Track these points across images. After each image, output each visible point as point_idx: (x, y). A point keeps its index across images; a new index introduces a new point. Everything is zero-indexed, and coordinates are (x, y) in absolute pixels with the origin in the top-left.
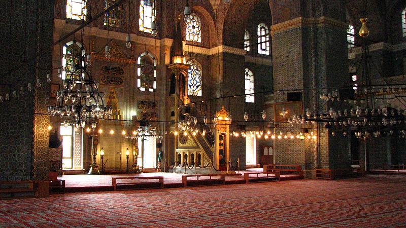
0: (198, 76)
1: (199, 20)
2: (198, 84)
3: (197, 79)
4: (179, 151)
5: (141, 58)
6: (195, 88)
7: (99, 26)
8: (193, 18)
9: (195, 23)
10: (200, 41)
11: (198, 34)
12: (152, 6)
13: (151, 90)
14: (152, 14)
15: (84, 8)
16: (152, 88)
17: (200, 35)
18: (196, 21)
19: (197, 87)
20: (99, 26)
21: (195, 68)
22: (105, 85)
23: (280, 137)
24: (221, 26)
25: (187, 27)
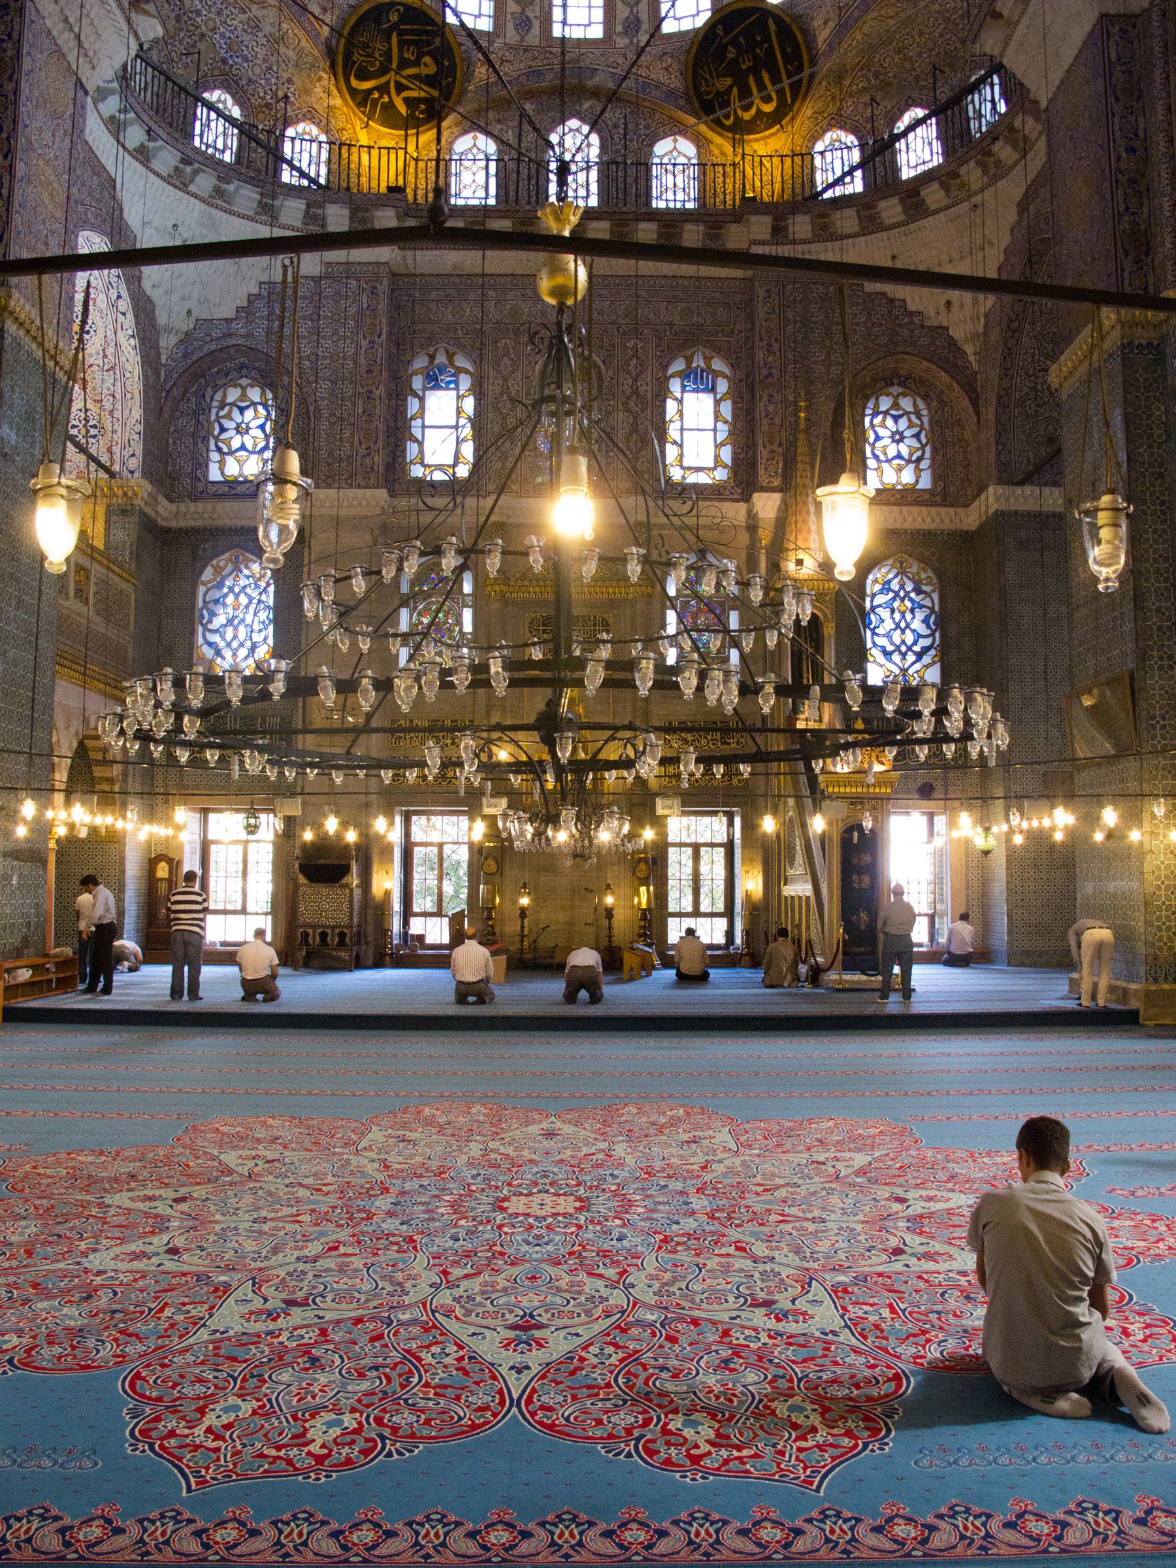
0: (920, 615)
1: (921, 405)
2: (925, 642)
3: (917, 625)
4: (789, 890)
6: (911, 658)
8: (896, 406)
9: (903, 423)
10: (925, 483)
11: (919, 460)
12: (713, 390)
14: (717, 416)
15: (465, 440)
17: (925, 464)
18: (908, 413)
19: (919, 656)
21: (909, 587)
24: (990, 413)
25: (866, 440)
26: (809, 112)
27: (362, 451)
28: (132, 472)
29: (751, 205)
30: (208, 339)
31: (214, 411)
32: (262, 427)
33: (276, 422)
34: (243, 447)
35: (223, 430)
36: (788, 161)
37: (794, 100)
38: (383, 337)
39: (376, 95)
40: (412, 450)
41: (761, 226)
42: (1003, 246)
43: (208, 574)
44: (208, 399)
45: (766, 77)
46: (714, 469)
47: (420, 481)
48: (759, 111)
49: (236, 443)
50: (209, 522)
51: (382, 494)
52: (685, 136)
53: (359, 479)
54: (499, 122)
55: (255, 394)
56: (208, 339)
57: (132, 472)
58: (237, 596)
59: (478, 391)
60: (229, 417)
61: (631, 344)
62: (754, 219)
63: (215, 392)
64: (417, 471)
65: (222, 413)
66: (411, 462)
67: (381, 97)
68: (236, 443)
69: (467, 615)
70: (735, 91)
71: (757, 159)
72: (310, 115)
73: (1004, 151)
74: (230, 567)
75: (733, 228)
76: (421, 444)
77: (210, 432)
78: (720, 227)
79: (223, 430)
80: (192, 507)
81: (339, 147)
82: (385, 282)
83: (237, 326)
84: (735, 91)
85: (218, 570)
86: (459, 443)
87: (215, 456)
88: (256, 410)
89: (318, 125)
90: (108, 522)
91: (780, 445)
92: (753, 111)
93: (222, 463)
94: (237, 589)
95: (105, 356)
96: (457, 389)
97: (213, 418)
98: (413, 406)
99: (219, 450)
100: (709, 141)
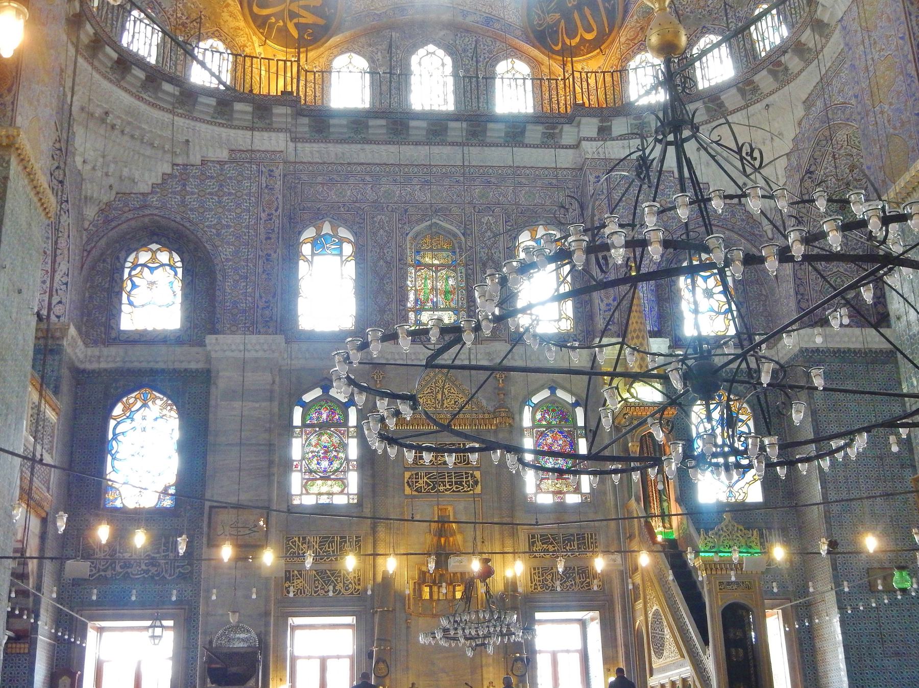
5: (536, 408)
13: (572, 499)
16: (577, 490)
26: (623, 39)
27: (261, 304)
28: (58, 317)
29: (580, 110)
30: (127, 209)
31: (127, 271)
35: (134, 286)
36: (608, 78)
37: (611, 31)
38: (280, 210)
39: (273, 20)
41: (590, 126)
42: (793, 136)
43: (118, 410)
44: (122, 261)
45: (587, 11)
46: (560, 320)
48: (582, 38)
50: (119, 365)
51: (280, 339)
52: (520, 59)
53: (260, 326)
54: (370, 45)
55: (164, 257)
56: (127, 209)
57: (58, 317)
59: (360, 255)
61: (485, 220)
62: (584, 120)
63: (128, 256)
65: (133, 273)
67: (277, 21)
70: (562, 23)
71: (584, 75)
72: (217, 34)
73: (792, 62)
74: (139, 404)
75: (566, 128)
77: (122, 289)
78: (554, 128)
79: (134, 286)
80: (106, 351)
81: (240, 58)
82: (281, 166)
83: (154, 200)
84: (563, 21)
85: (127, 408)
87: (125, 308)
89: (224, 42)
91: (614, 300)
92: (577, 39)
96: (341, 254)
97: (126, 275)
98: (302, 266)
99: (131, 303)
100: (540, 63)
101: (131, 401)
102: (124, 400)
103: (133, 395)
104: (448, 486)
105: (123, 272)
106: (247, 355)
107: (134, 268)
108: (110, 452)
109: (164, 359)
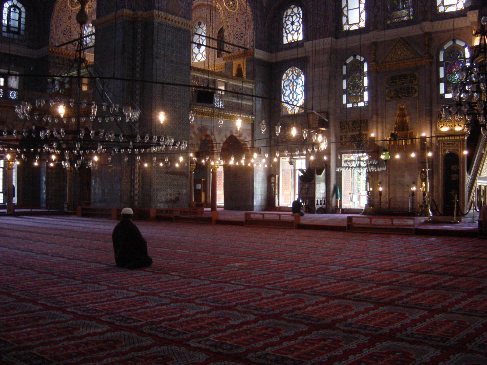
7: (380, 27)
15: (361, 12)
20: (380, 27)
22: (391, 101)
23: (243, 162)
31: (284, 19)
32: (298, 22)
33: (302, 19)
34: (293, 30)
35: (287, 25)
40: (344, 20)
47: (348, 31)
49: (291, 29)
55: (296, 10)
58: (293, 83)
60: (288, 20)
63: (284, 13)
64: (346, 28)
65: (286, 19)
66: (344, 25)
68: (291, 29)
69: (366, 79)
76: (347, 17)
77: (283, 27)
79: (287, 25)
86: (360, 14)
87: (285, 35)
88: (296, 16)
90: (247, 65)
93: (287, 37)
94: (293, 80)
95: (241, 10)
97: (284, 21)
99: (286, 32)
101: (288, 72)
102: (286, 72)
103: (289, 70)
104: (403, 95)
105: (283, 19)
106: (325, 47)
107: (286, 17)
108: (283, 94)
109: (299, 53)
